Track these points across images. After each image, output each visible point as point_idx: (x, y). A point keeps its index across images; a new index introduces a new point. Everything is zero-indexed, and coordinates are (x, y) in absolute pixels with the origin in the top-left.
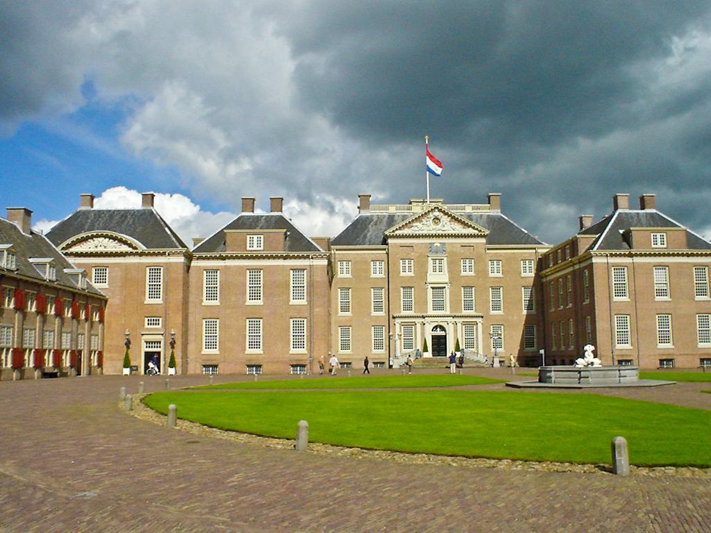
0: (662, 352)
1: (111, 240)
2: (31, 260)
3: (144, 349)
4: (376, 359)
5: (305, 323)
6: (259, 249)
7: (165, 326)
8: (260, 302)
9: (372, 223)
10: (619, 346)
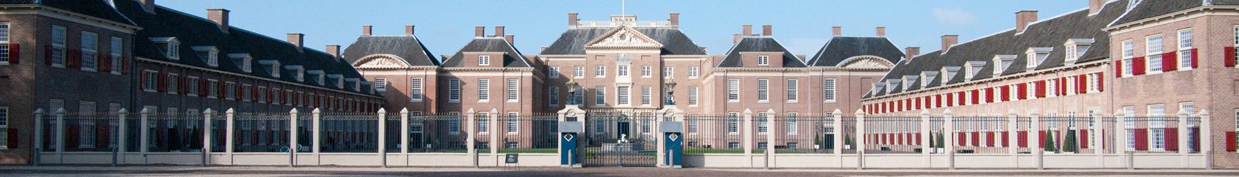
9: (577, 36)
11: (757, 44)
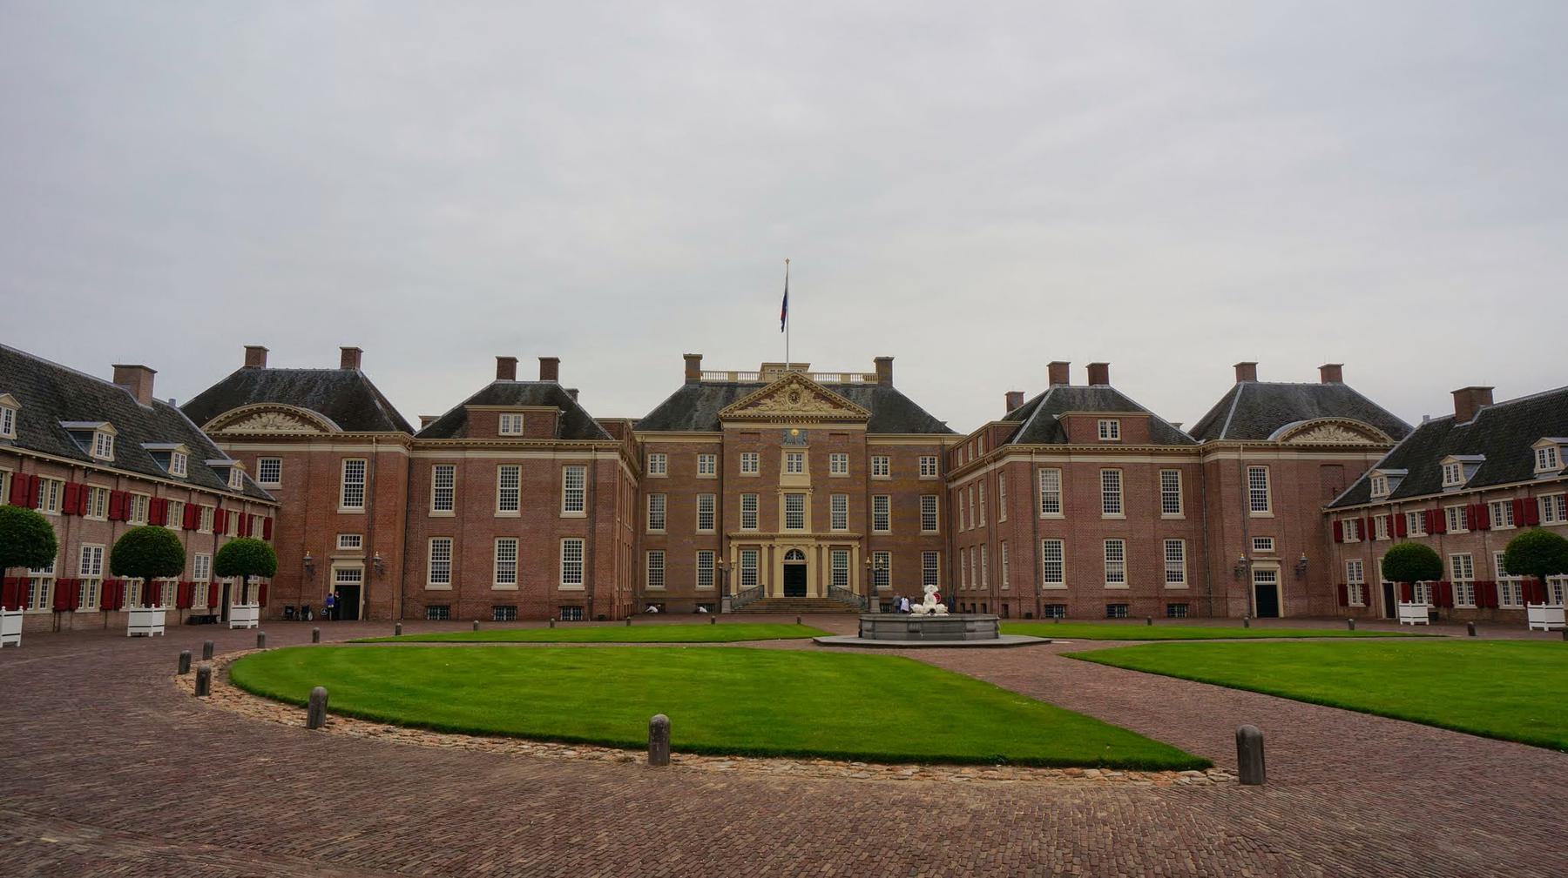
0: (1110, 594)
1: (288, 418)
2: (145, 446)
3: (334, 581)
4: (700, 598)
5: (583, 545)
6: (516, 434)
7: (369, 549)
8: (515, 513)
10: (1047, 585)
11: (1084, 398)
